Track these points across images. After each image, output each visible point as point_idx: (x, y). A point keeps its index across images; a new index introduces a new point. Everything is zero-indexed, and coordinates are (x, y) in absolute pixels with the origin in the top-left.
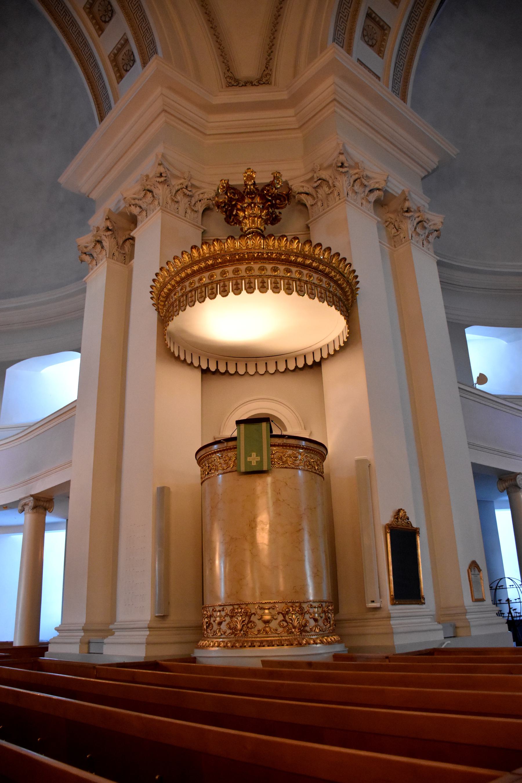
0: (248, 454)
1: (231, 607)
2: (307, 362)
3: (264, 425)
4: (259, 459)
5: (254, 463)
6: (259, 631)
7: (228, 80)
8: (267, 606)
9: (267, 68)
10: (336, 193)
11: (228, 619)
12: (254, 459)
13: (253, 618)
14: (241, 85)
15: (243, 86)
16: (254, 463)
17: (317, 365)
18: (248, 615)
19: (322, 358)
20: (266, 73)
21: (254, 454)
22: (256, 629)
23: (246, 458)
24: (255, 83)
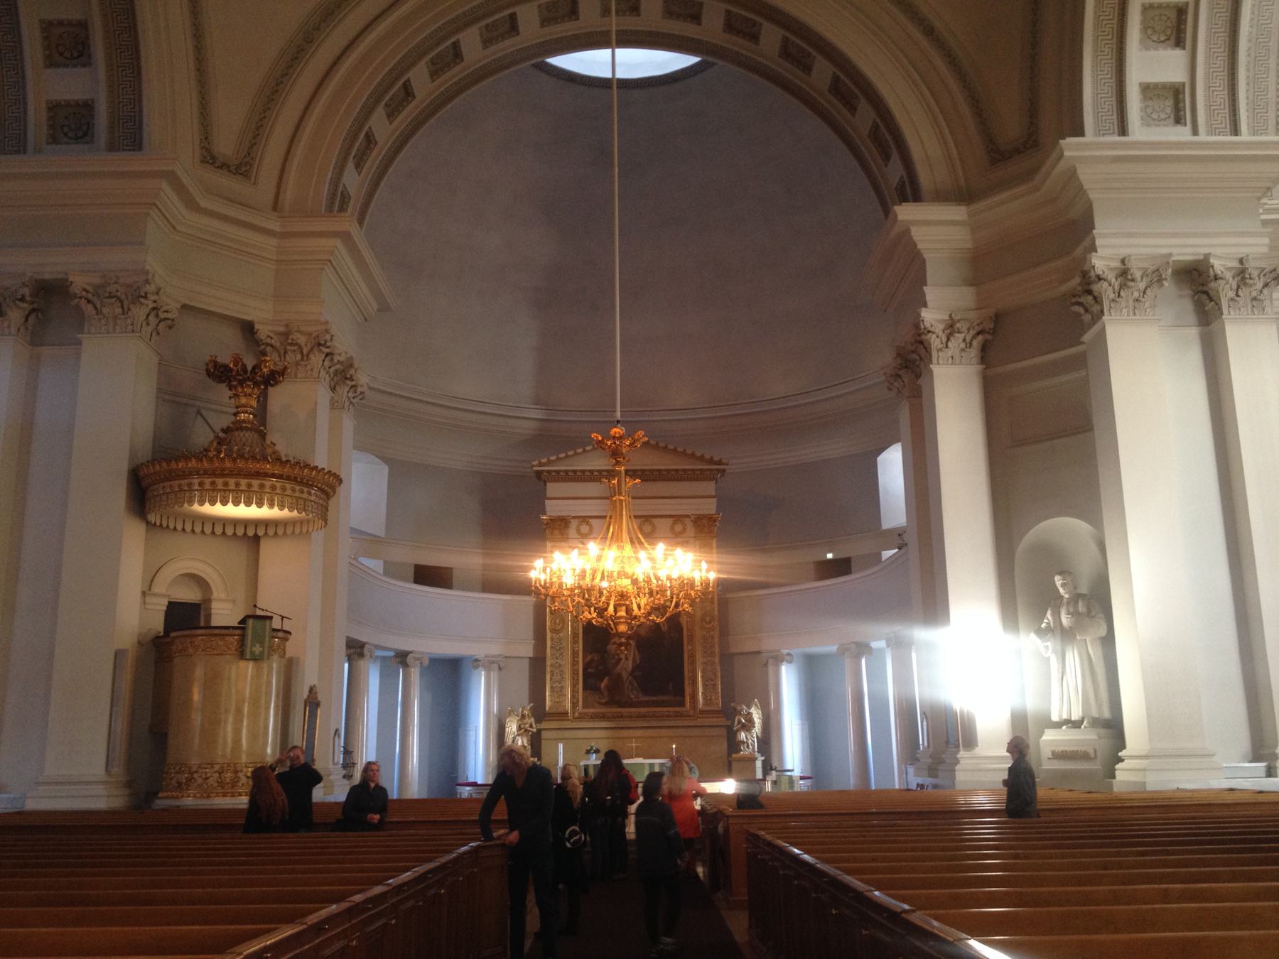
0: (253, 645)
1: (220, 766)
2: (247, 532)
3: (268, 622)
4: (261, 649)
5: (257, 653)
6: (243, 784)
7: (204, 151)
8: (250, 765)
9: (249, 154)
10: (309, 367)
11: (216, 775)
12: (257, 649)
13: (241, 775)
14: (217, 165)
15: (218, 167)
16: (257, 653)
17: (256, 538)
18: (236, 772)
19: (266, 534)
20: (246, 160)
21: (258, 645)
22: (241, 782)
23: (251, 648)
24: (232, 168)
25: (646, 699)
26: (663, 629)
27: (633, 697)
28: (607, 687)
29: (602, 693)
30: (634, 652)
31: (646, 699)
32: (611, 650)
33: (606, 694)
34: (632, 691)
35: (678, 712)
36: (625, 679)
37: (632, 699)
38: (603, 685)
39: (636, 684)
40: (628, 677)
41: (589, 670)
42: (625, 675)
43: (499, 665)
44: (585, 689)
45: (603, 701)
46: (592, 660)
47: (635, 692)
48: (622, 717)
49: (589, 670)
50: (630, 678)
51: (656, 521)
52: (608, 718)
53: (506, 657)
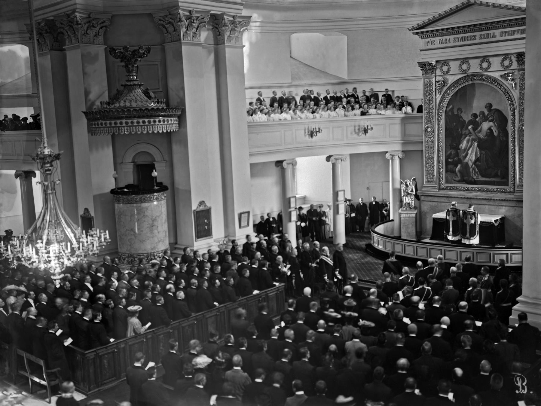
25: (484, 179)
26: (495, 134)
27: (475, 177)
28: (459, 171)
29: (457, 175)
30: (476, 148)
31: (484, 179)
32: (462, 147)
33: (459, 175)
34: (475, 175)
35: (504, 189)
36: (470, 167)
37: (474, 179)
38: (457, 169)
39: (477, 170)
40: (472, 165)
41: (449, 160)
42: (470, 164)
43: (399, 157)
44: (447, 171)
45: (457, 179)
46: (451, 154)
47: (476, 175)
48: (467, 190)
49: (449, 160)
50: (473, 165)
51: (491, 59)
52: (460, 190)
53: (403, 151)
